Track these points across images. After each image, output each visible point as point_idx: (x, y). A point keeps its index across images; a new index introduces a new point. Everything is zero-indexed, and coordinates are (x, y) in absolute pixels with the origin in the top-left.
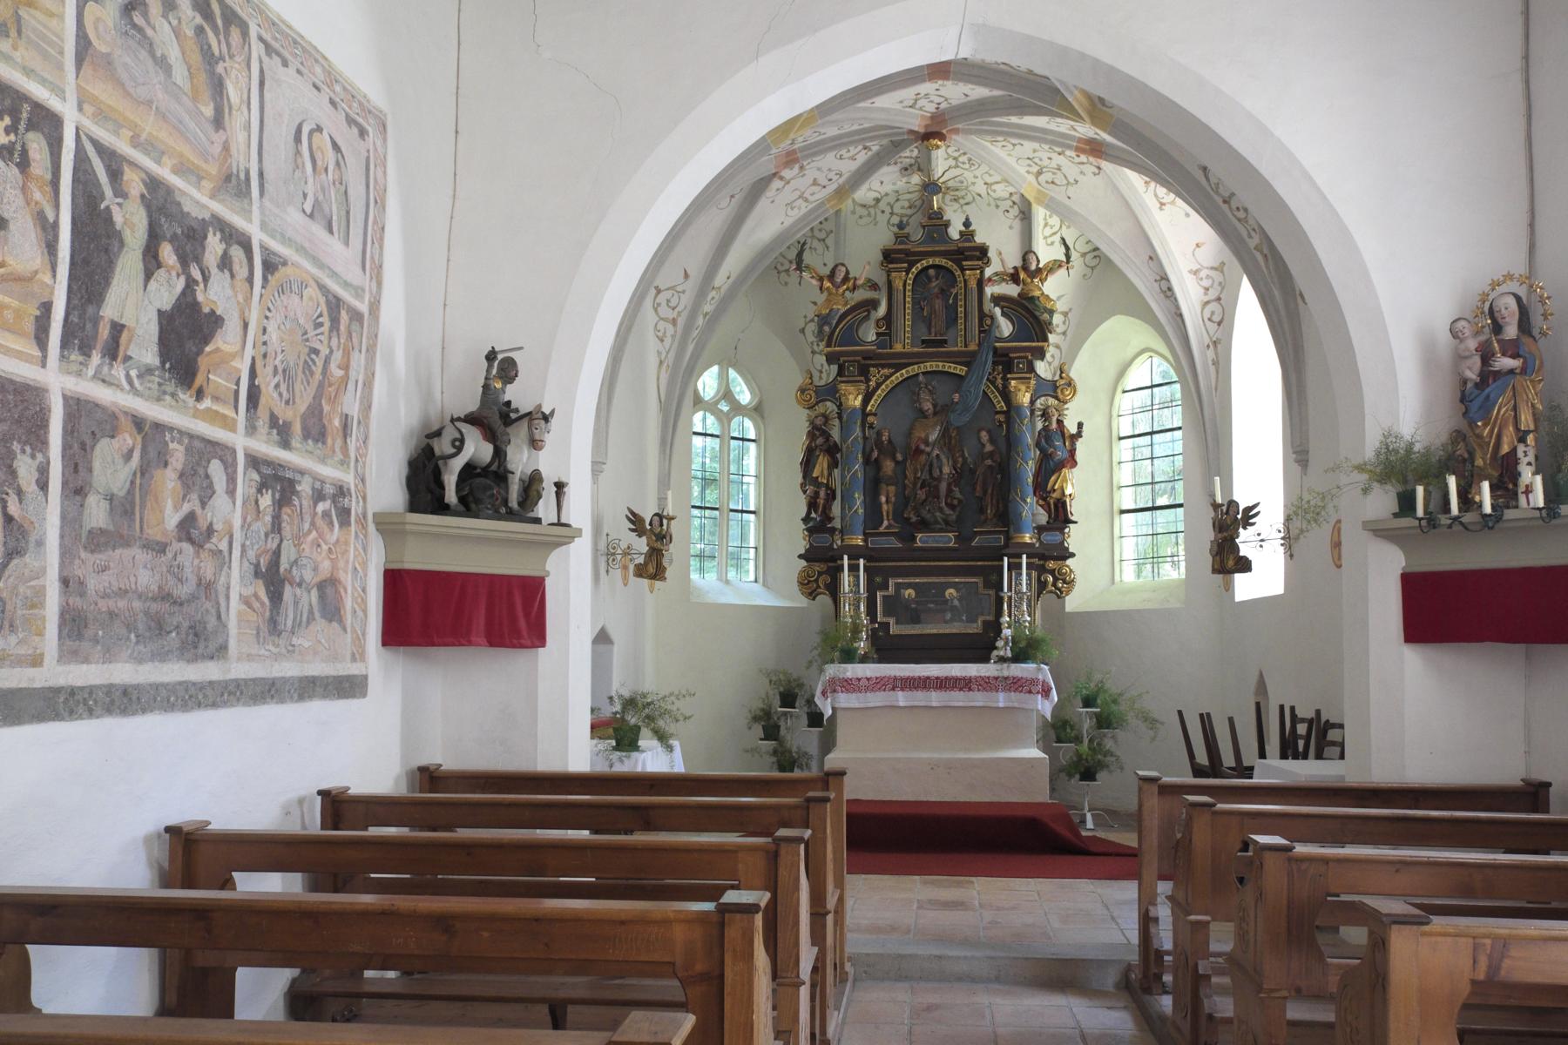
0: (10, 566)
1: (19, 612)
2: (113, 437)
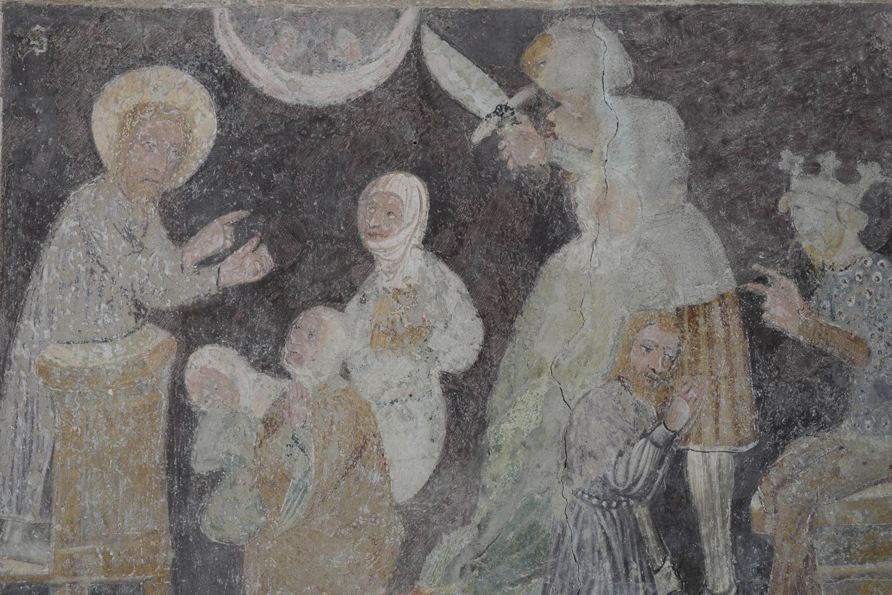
0: (785, 456)
1: (825, 571)
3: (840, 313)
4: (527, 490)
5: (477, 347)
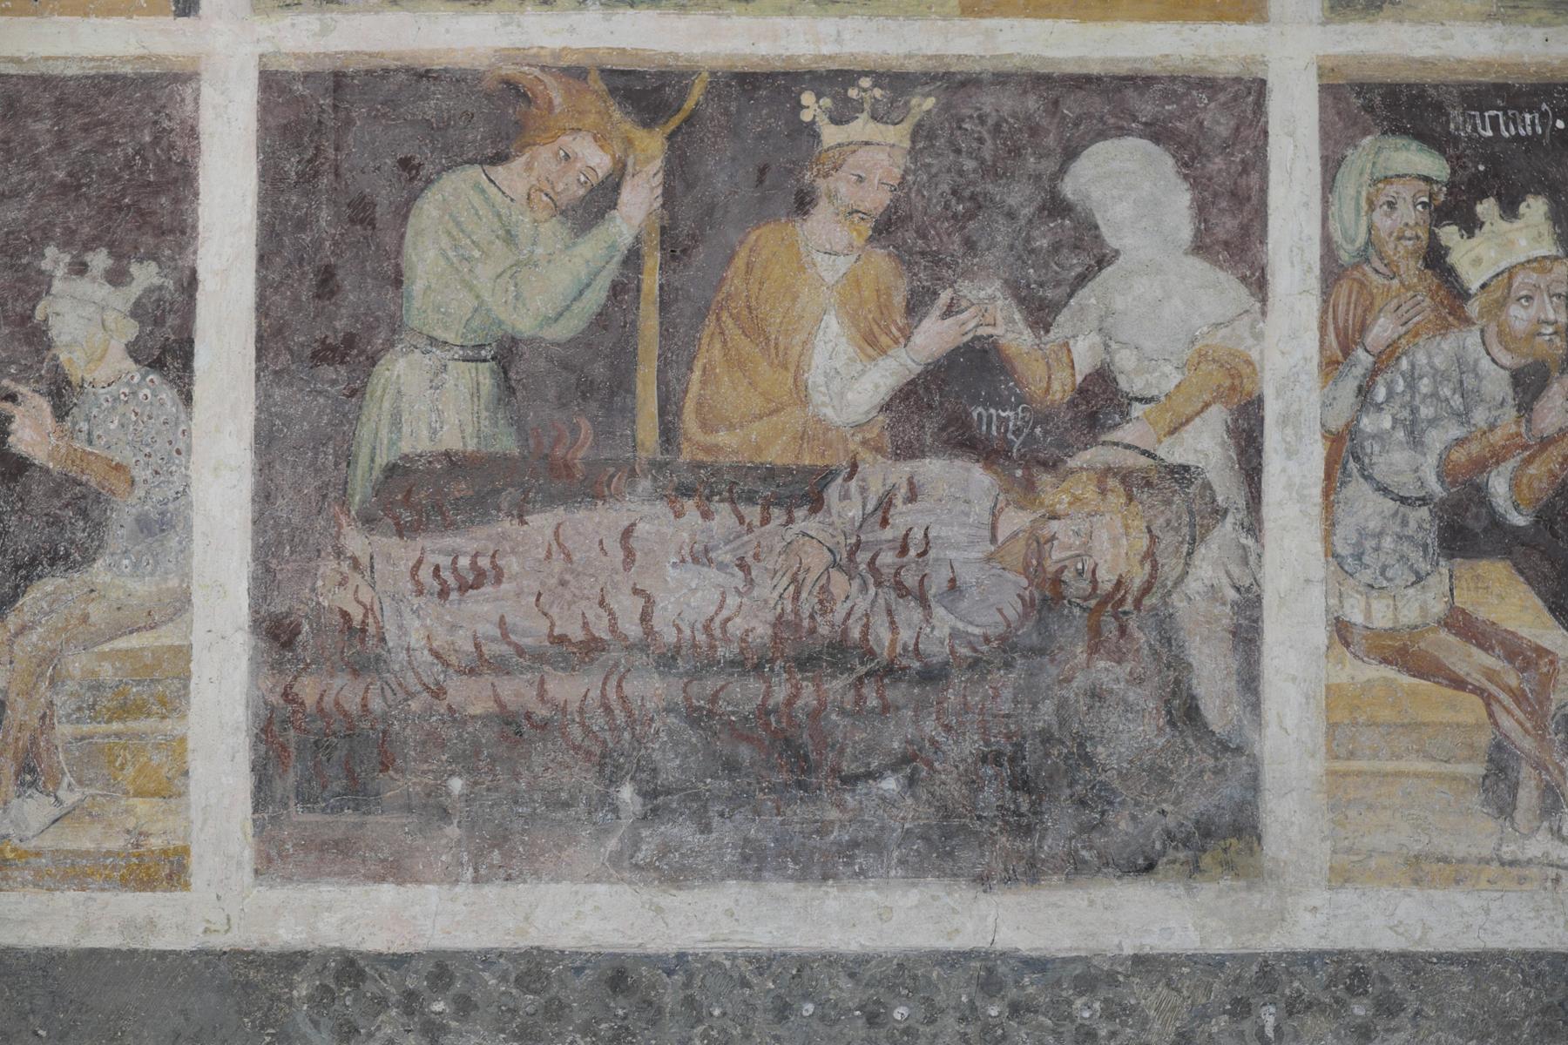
0: (25, 601)
1: (64, 730)
2: (500, 158)
3: (99, 437)
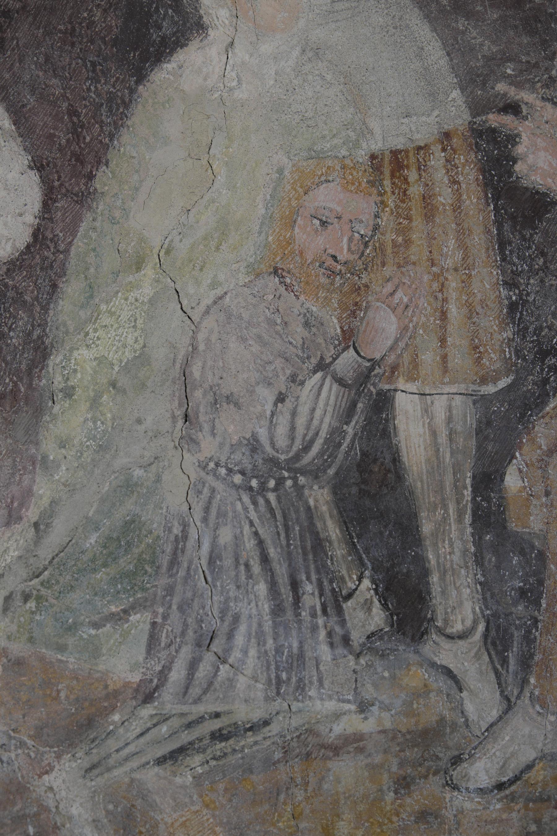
4: (121, 461)
5: (30, 219)
